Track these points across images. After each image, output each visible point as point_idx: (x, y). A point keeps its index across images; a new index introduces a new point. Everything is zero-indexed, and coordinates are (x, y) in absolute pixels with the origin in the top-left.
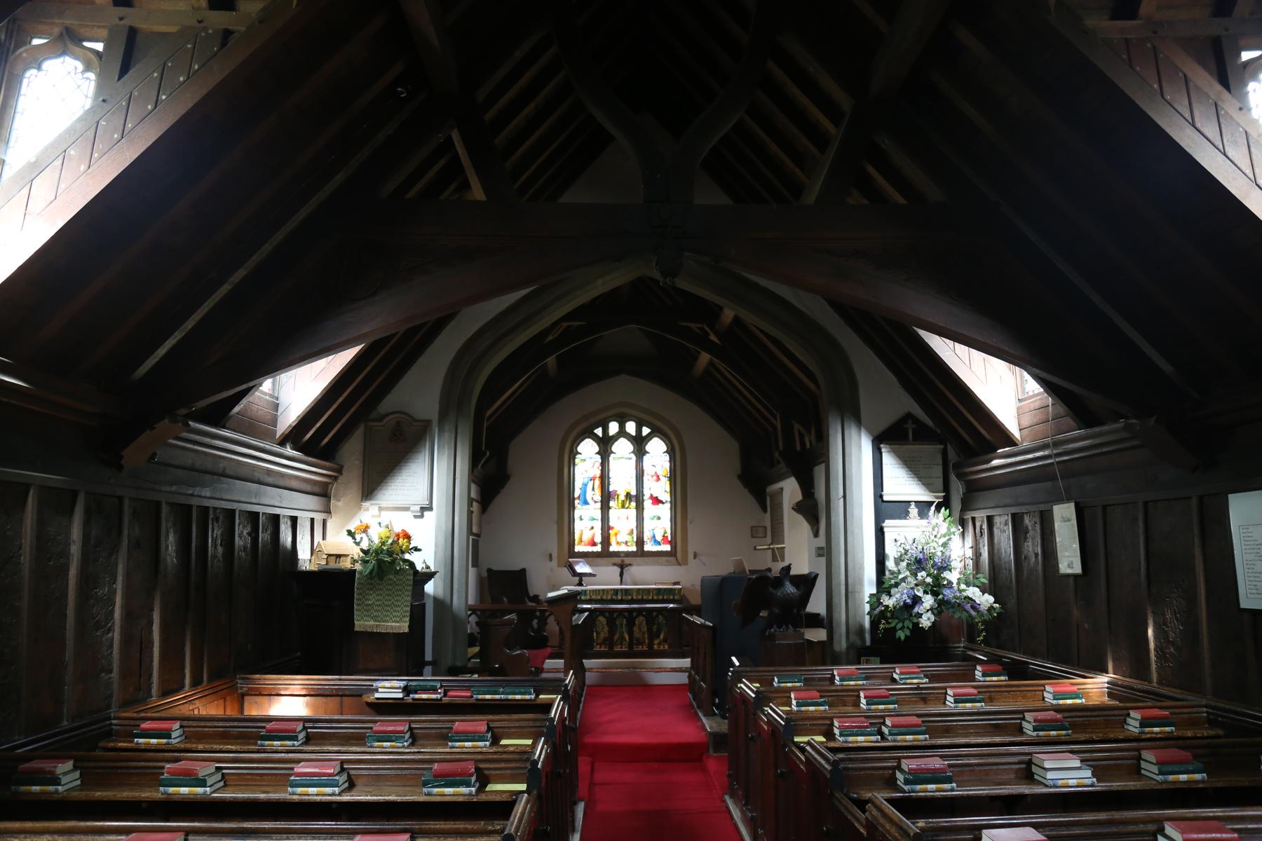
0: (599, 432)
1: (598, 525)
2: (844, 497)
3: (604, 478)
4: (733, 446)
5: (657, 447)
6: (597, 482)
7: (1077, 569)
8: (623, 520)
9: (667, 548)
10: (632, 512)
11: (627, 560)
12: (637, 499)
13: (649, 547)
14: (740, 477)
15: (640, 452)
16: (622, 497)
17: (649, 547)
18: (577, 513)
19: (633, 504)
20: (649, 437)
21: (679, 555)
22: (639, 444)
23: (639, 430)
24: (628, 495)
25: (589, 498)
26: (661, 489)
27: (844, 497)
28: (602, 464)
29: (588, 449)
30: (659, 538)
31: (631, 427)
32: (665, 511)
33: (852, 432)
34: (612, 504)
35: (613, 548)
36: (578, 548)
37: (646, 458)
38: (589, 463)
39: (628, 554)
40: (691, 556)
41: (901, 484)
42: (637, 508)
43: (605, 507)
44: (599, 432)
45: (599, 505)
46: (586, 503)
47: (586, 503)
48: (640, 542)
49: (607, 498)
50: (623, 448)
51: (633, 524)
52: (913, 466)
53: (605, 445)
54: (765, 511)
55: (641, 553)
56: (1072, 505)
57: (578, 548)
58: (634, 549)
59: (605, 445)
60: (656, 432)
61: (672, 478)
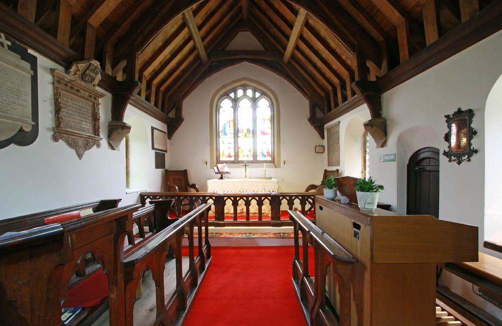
0: (232, 95)
1: (232, 146)
4: (306, 103)
5: (264, 104)
6: (232, 124)
9: (269, 159)
10: (251, 139)
13: (260, 158)
16: (245, 131)
18: (221, 140)
19: (251, 135)
20: (260, 98)
21: (276, 161)
22: (254, 100)
23: (254, 94)
24: (248, 131)
25: (227, 132)
29: (226, 104)
30: (265, 153)
31: (250, 92)
32: (268, 139)
34: (240, 135)
35: (240, 159)
36: (222, 159)
37: (257, 109)
45: (233, 135)
47: (225, 134)
48: (255, 155)
49: (236, 133)
53: (235, 101)
54: (323, 138)
57: (222, 159)
58: (251, 159)
59: (235, 101)
60: (263, 94)
61: (272, 119)
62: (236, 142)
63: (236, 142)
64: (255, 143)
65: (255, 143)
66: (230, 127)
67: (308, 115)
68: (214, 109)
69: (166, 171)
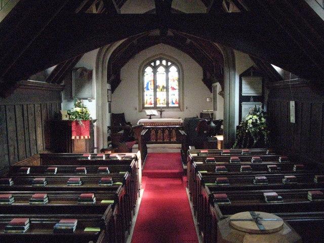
0: (153, 64)
2: (229, 94)
3: (155, 81)
4: (201, 69)
5: (174, 70)
7: (294, 122)
8: (161, 96)
9: (177, 105)
10: (164, 93)
11: (163, 110)
12: (166, 88)
13: (171, 105)
14: (203, 80)
15: (167, 71)
16: (161, 88)
17: (171, 105)
18: (145, 93)
19: (165, 90)
20: (171, 66)
21: (181, 108)
22: (167, 68)
24: (163, 87)
25: (149, 88)
26: (174, 84)
27: (229, 94)
28: (154, 76)
29: (149, 70)
30: (174, 102)
31: (164, 62)
32: (176, 92)
33: (232, 72)
34: (158, 90)
35: (158, 106)
36: (146, 106)
37: (169, 73)
39: (163, 108)
41: (247, 91)
42: (166, 91)
43: (155, 91)
45: (153, 90)
46: (148, 89)
47: (148, 89)
48: (168, 103)
49: (156, 88)
51: (165, 97)
52: (252, 85)
53: (155, 68)
55: (168, 107)
56: (294, 102)
57: (146, 106)
58: (165, 106)
59: (155, 68)
60: (173, 64)
61: (179, 80)
64: (168, 95)
65: (168, 95)
67: (202, 77)
68: (142, 73)
69: (113, 114)
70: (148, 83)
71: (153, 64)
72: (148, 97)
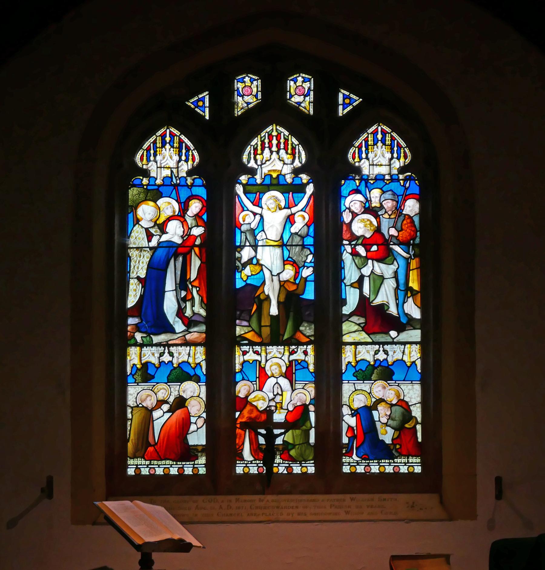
1: (194, 392)
3: (219, 241)
5: (379, 157)
6: (196, 263)
9: (413, 465)
10: (307, 355)
15: (329, 170)
20: (358, 122)
23: (325, 97)
29: (167, 159)
30: (387, 436)
38: (168, 205)
40: (485, 488)
42: (318, 342)
43: (220, 345)
44: (203, 104)
49: (228, 308)
50: (274, 157)
62: (220, 378)
63: (220, 378)
64: (328, 378)
65: (328, 378)
66: (183, 283)
70: (154, 283)
71: (203, 104)
72: (162, 386)
